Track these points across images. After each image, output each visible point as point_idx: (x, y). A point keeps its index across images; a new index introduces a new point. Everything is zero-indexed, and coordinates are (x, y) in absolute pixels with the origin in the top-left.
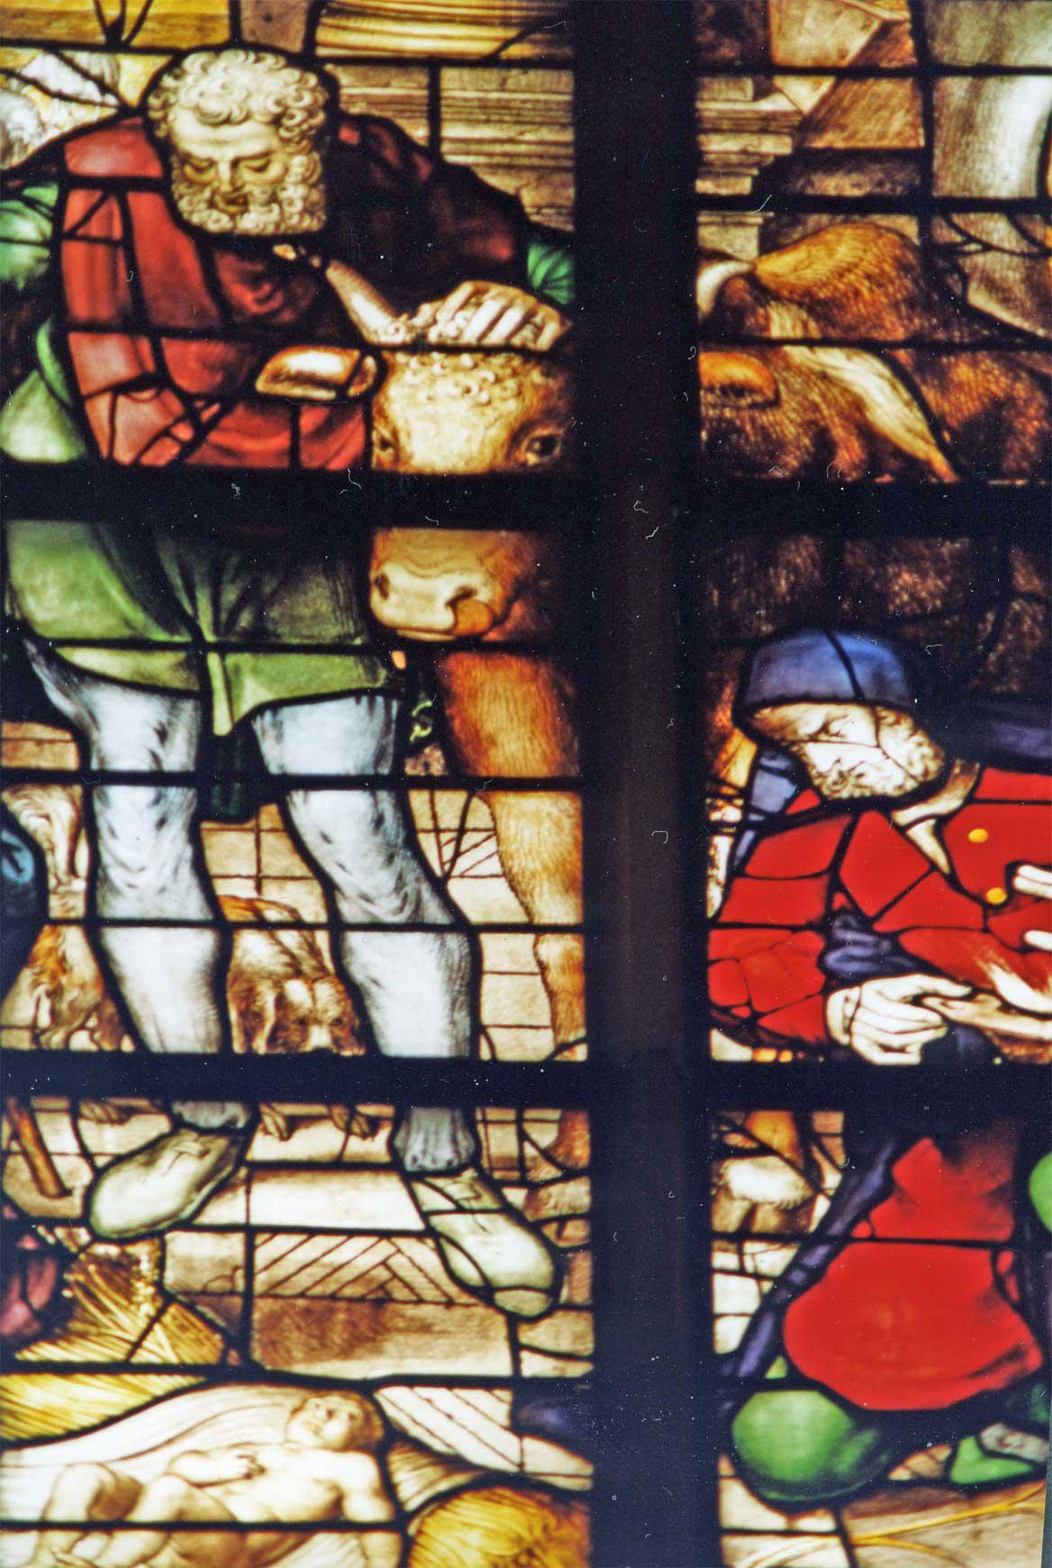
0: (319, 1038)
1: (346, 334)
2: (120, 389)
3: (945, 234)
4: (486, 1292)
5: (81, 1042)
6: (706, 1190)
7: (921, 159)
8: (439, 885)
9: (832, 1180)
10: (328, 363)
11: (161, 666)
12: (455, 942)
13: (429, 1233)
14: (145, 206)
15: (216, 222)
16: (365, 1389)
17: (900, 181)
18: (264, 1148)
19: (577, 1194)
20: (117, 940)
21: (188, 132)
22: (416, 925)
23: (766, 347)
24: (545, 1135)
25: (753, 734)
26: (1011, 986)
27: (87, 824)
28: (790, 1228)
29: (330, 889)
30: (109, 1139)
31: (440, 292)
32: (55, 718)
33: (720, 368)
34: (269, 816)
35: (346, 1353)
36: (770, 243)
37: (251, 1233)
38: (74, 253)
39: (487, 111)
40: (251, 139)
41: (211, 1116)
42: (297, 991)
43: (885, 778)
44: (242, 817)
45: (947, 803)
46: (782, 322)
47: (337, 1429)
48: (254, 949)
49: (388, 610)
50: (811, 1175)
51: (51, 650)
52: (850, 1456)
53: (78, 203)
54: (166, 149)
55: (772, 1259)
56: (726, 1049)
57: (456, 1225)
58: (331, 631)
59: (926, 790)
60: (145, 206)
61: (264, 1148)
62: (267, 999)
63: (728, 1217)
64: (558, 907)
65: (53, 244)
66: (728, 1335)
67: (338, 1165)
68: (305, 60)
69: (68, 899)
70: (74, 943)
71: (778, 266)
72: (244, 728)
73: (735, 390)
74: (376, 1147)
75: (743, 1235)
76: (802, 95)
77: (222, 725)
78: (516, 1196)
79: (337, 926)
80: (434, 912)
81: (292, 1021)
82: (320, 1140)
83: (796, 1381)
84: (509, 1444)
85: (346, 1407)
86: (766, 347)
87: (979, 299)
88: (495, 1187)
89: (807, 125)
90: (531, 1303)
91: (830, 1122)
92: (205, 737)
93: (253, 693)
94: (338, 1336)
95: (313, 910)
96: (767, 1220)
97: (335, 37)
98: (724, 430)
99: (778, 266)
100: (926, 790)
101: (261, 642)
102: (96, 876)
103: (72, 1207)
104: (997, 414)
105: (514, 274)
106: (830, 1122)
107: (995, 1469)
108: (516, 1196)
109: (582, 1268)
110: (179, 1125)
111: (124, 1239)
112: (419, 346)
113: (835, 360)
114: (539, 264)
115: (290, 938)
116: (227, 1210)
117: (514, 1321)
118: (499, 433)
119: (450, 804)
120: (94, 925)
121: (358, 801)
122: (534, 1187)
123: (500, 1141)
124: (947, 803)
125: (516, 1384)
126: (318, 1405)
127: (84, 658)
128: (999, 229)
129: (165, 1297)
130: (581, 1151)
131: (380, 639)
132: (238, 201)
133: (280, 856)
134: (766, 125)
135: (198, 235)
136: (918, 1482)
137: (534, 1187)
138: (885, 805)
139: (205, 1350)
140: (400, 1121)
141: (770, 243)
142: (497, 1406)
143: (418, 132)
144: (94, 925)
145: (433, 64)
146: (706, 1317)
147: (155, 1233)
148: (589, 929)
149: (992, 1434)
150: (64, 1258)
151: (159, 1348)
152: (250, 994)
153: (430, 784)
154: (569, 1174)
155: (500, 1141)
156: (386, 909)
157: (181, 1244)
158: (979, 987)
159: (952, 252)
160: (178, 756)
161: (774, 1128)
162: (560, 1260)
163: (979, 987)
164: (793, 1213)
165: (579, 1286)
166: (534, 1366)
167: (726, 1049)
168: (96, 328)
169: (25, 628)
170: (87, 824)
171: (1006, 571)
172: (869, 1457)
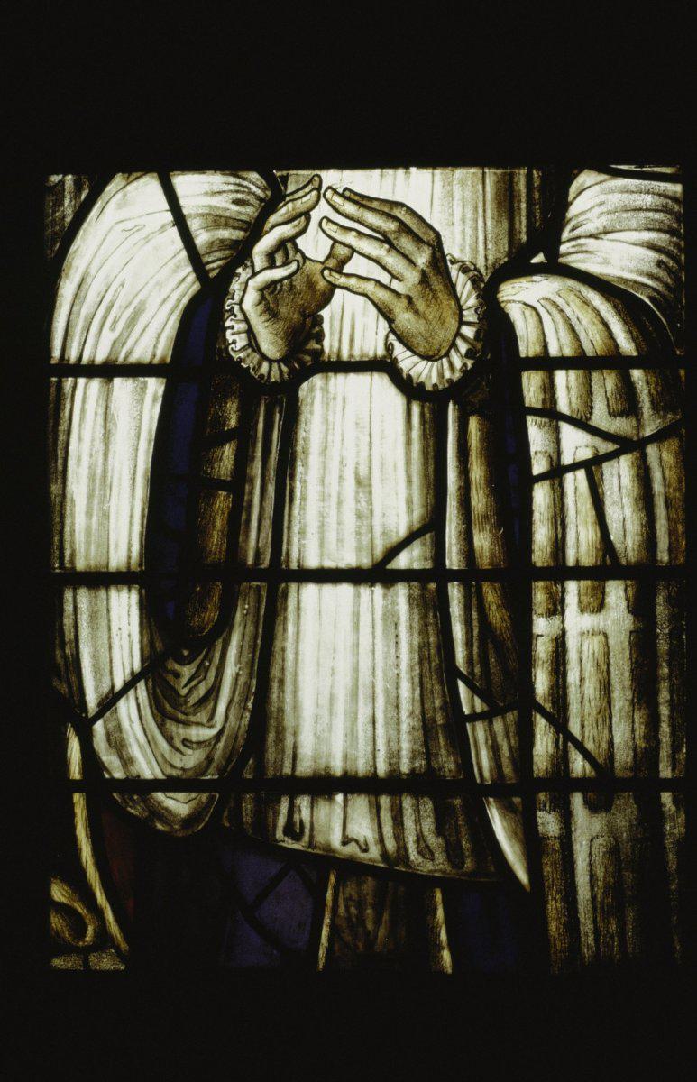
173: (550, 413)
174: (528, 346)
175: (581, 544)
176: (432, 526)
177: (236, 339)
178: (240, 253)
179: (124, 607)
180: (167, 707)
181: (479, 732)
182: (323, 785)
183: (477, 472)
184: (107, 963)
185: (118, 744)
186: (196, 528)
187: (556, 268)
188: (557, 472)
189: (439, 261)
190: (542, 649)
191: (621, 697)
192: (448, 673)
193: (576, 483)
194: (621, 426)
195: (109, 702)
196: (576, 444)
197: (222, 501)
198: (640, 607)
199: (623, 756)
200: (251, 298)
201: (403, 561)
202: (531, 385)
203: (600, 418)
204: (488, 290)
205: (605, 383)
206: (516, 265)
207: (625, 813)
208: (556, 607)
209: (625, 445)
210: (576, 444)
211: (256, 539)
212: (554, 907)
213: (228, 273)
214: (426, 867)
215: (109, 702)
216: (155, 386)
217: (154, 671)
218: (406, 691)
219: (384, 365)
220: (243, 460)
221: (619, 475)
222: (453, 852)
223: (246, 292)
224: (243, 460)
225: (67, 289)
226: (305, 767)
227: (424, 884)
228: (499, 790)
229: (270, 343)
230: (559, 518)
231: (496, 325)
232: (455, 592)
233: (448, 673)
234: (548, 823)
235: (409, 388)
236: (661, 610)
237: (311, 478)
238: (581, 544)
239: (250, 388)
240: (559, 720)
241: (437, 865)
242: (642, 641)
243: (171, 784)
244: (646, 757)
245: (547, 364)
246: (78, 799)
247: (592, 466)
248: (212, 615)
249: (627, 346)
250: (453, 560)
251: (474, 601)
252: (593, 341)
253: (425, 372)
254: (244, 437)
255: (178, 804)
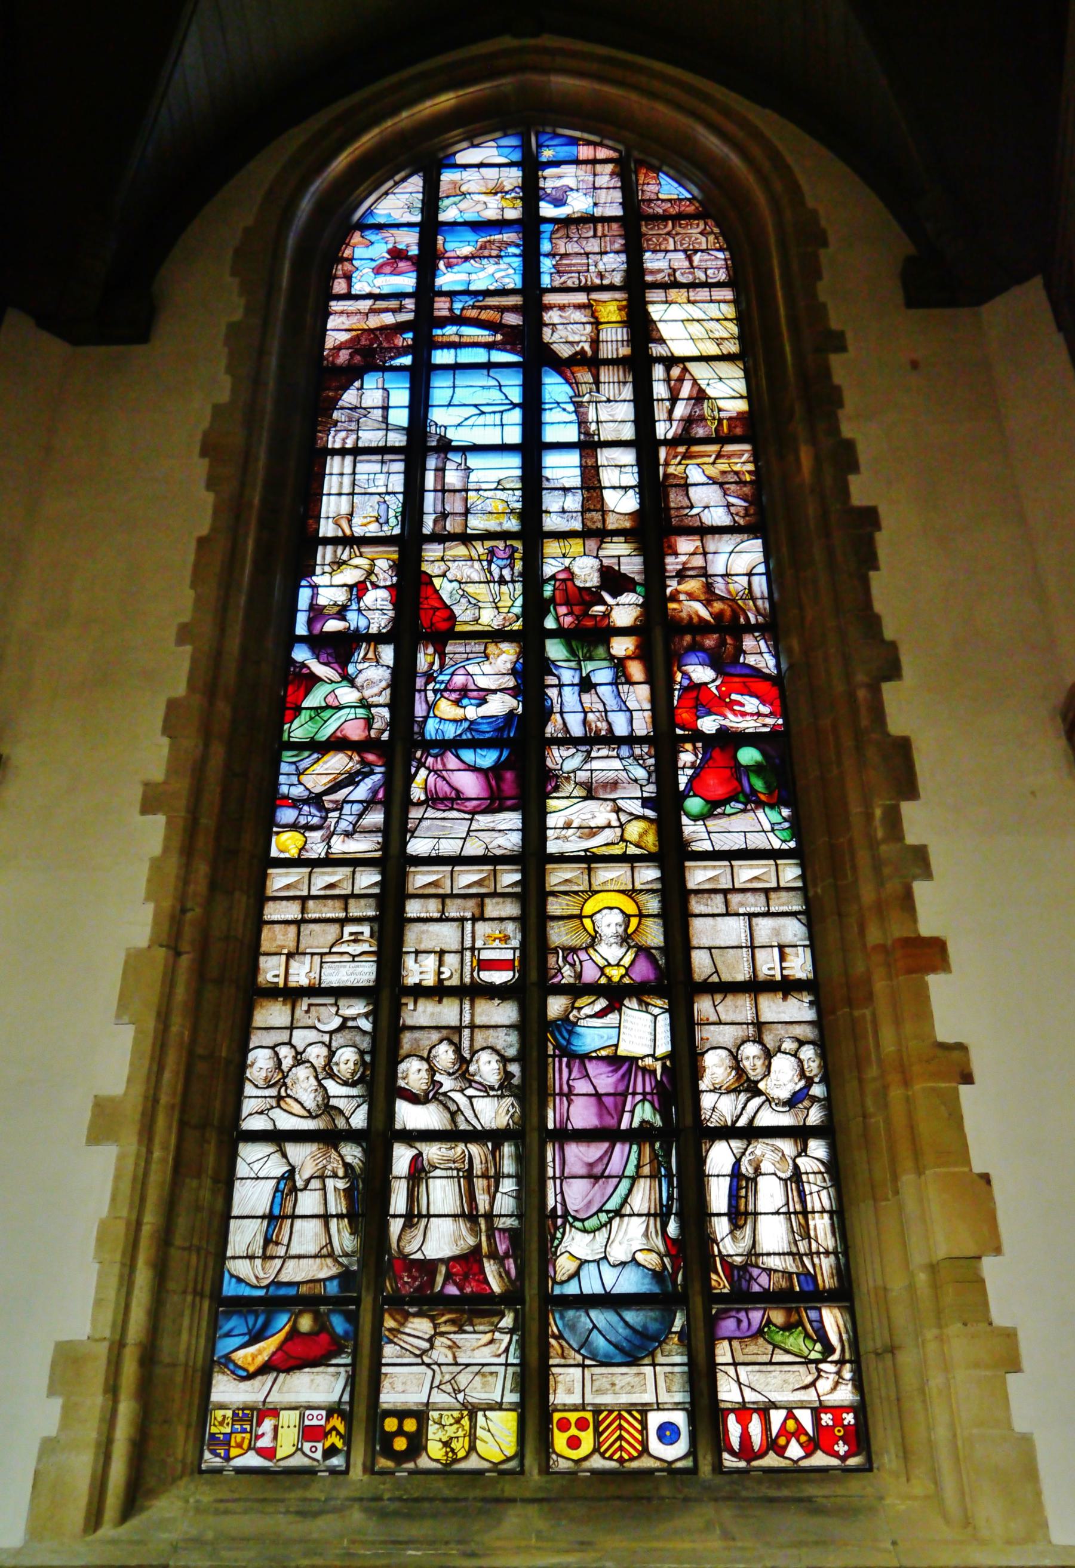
0: (603, 733)
1: (604, 603)
2: (565, 615)
3: (710, 581)
4: (636, 781)
5: (560, 735)
6: (676, 759)
7: (705, 568)
8: (624, 703)
9: (700, 756)
10: (601, 608)
11: (573, 664)
12: (628, 714)
13: (625, 769)
14: (569, 583)
15: (582, 585)
16: (614, 800)
17: (701, 572)
18: (593, 754)
19: (652, 761)
20: (565, 715)
21: (576, 570)
22: (621, 710)
23: (679, 602)
24: (646, 750)
25: (681, 672)
26: (730, 716)
27: (560, 694)
28: (693, 766)
29: (604, 704)
30: (565, 754)
31: (621, 595)
32: (554, 675)
33: (672, 605)
34: (593, 691)
35: (610, 793)
36: (679, 583)
37: (592, 770)
38: (557, 592)
39: (628, 564)
40: (587, 571)
41: (584, 748)
42: (599, 724)
43: (706, 679)
44: (587, 691)
45: (718, 682)
46: (682, 597)
47: (609, 808)
48: (590, 716)
49: (613, 652)
50: (696, 755)
51: (553, 662)
52: (706, 810)
53: (558, 583)
54: (572, 574)
55: (690, 772)
56: (679, 732)
57: (629, 768)
58: (603, 656)
59: (714, 681)
60: (569, 583)
61: (593, 754)
62: (593, 726)
63: (680, 764)
64: (648, 706)
65: (554, 591)
66: (682, 787)
67: (607, 757)
68: (597, 557)
69: (557, 709)
70: (558, 716)
71: (681, 588)
72: (588, 675)
73: (674, 609)
74: (614, 753)
75: (683, 768)
76: (683, 559)
77: (584, 675)
78: (641, 762)
79: (606, 711)
80: (624, 708)
81: (598, 730)
82: (604, 752)
83: (695, 795)
84: (641, 810)
85: (610, 804)
86: (679, 602)
87: (717, 591)
88: (637, 760)
89: (684, 564)
90: (644, 782)
91: (699, 745)
92: (581, 677)
93: (589, 668)
94: (608, 790)
95: (602, 709)
96: (688, 765)
97: (601, 553)
98: (673, 617)
99: (681, 588)
100: (714, 681)
101: (591, 659)
102: (562, 704)
103: (559, 767)
104: (722, 612)
105: (634, 591)
106: (699, 745)
107: (733, 811)
108: (641, 762)
109: (654, 775)
110: (578, 750)
111: (568, 773)
112: (618, 604)
113: (692, 603)
114: (639, 589)
115: (597, 714)
116: (587, 766)
117: (641, 786)
118: (633, 619)
119: (626, 687)
120: (562, 713)
121: (609, 687)
122: (644, 760)
123: (637, 751)
124: (718, 682)
125: (642, 798)
126: (606, 803)
127: (559, 663)
128: (719, 579)
129: (576, 784)
130: (653, 752)
131: (612, 658)
132: (586, 581)
133: (595, 698)
134: (677, 564)
135: (579, 588)
136: (719, 814)
137: (644, 760)
138: (706, 684)
139: (583, 793)
140: (619, 748)
141: (679, 583)
142: (639, 802)
143: (617, 568)
144: (562, 713)
145: (619, 557)
146: (678, 784)
147: (574, 771)
148: (653, 710)
149: (732, 804)
150: (557, 777)
151: (575, 793)
152: (590, 725)
153: (622, 684)
154: (651, 757)
155: (637, 751)
156: (615, 708)
157: (578, 773)
158: (725, 717)
159: (711, 584)
160: (576, 681)
161: (689, 746)
162: (650, 774)
163: (725, 717)
164: (693, 763)
165: (653, 779)
166: (645, 795)
167: (679, 732)
168: (561, 605)
169: (548, 659)
170: (560, 694)
171: (725, 640)
172: (709, 810)
173: (809, 1182)
174: (803, 1170)
175: (818, 1207)
176: (787, 1204)
177: (743, 1170)
178: (743, 1154)
179: (725, 1220)
180: (734, 1239)
181: (800, 1244)
182: (769, 1254)
183: (795, 1193)
184: (726, 1291)
185: (725, 1248)
186: (737, 1207)
187: (806, 1155)
188: (811, 1193)
189: (783, 1155)
190: (812, 1227)
191: (829, 1235)
192: (793, 1232)
193: (815, 1195)
194: (824, 1185)
195: (722, 1239)
196: (815, 1188)
197: (743, 1200)
198: (831, 1218)
199: (831, 1249)
200: (746, 1163)
201: (781, 1210)
202: (804, 1177)
203: (819, 1183)
204: (794, 1161)
205: (819, 1177)
206: (799, 1155)
207: (832, 1258)
208: (814, 1219)
209: (824, 1188)
210: (815, 1188)
211: (751, 1208)
212: (819, 1278)
213: (741, 1158)
214: (791, 1270)
215: (722, 1239)
216: (728, 1179)
217: (731, 1232)
218: (785, 1237)
219: (775, 1174)
220: (747, 1192)
221: (824, 1194)
222: (797, 1267)
223: (745, 1161)
224: (747, 1192)
225: (708, 1161)
226: (765, 1251)
227: (790, 1274)
228: (806, 1255)
229: (751, 1170)
230: (813, 1202)
231: (796, 1167)
232: (793, 1216)
233: (793, 1232)
234: (816, 1260)
235: (780, 1179)
236: (835, 1219)
237: (760, 1195)
238: (818, 1207)
239: (748, 1179)
240: (817, 1241)
241: (794, 1270)
242: (832, 1225)
243: (737, 1255)
244: (836, 1247)
245: (807, 1173)
246: (718, 1259)
247: (818, 1192)
248: (742, 1222)
249: (823, 1170)
250: (792, 1210)
251: (797, 1218)
252: (816, 1170)
253: (783, 1176)
254: (747, 1187)
255: (738, 1260)
